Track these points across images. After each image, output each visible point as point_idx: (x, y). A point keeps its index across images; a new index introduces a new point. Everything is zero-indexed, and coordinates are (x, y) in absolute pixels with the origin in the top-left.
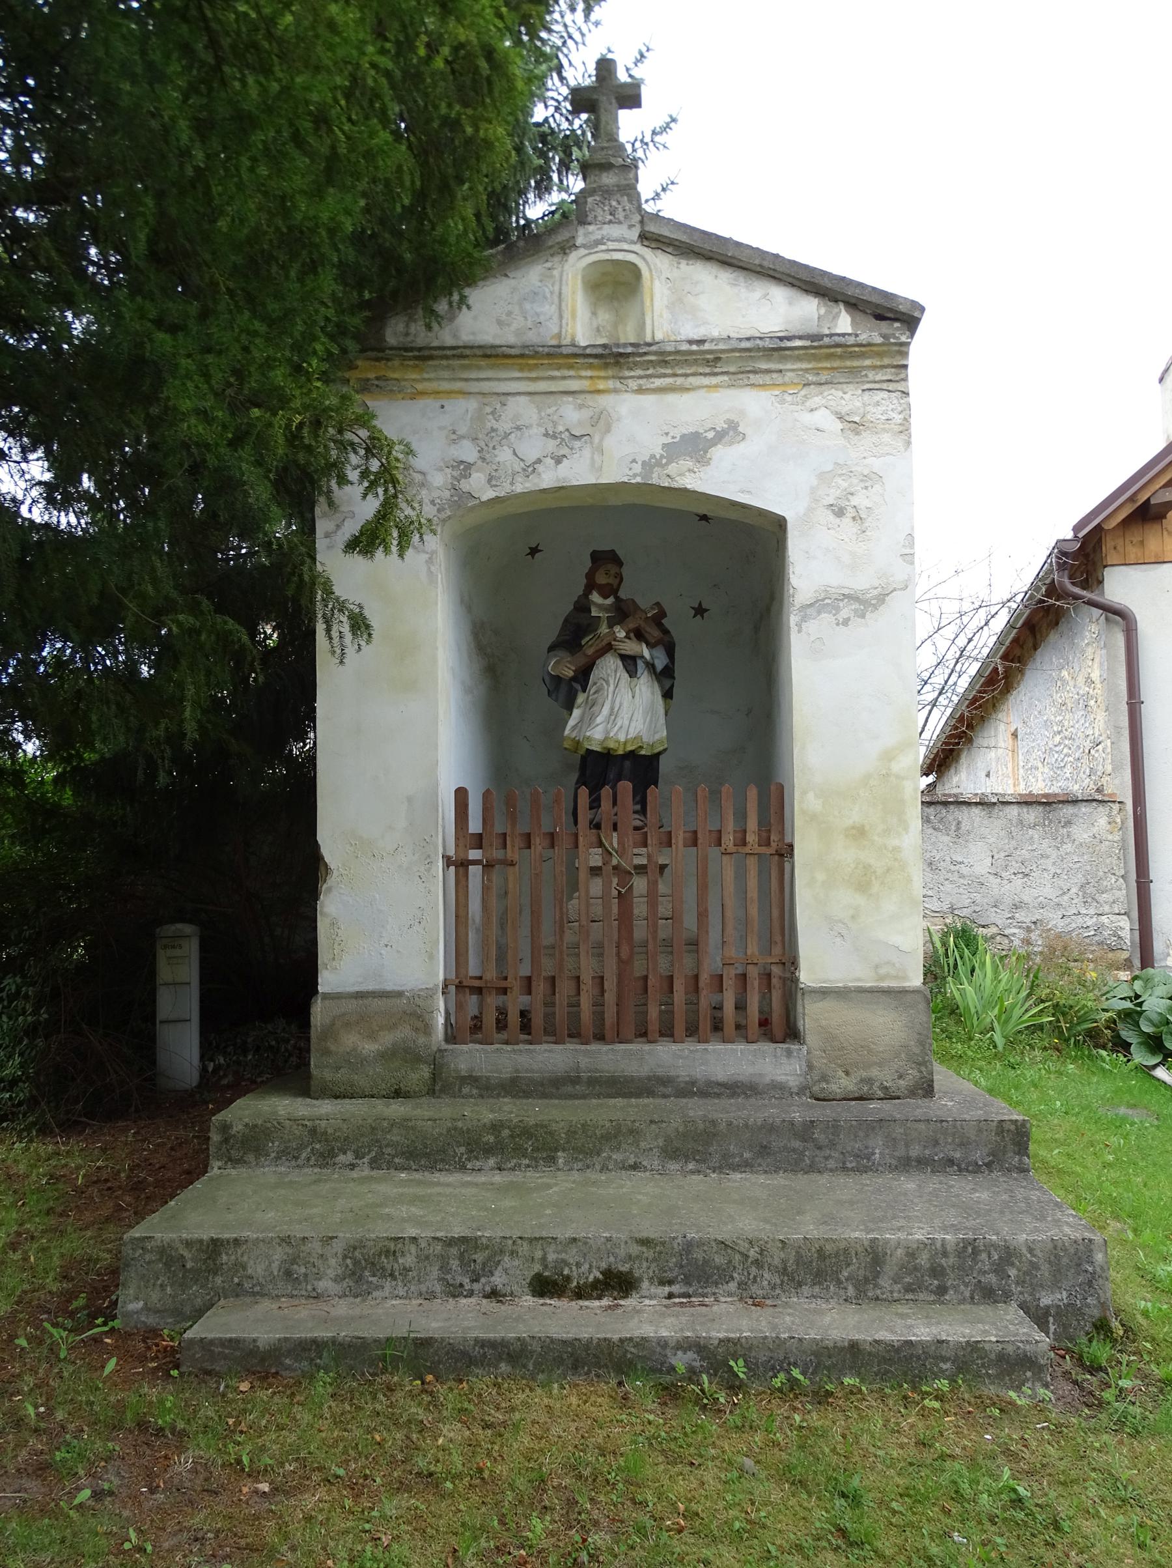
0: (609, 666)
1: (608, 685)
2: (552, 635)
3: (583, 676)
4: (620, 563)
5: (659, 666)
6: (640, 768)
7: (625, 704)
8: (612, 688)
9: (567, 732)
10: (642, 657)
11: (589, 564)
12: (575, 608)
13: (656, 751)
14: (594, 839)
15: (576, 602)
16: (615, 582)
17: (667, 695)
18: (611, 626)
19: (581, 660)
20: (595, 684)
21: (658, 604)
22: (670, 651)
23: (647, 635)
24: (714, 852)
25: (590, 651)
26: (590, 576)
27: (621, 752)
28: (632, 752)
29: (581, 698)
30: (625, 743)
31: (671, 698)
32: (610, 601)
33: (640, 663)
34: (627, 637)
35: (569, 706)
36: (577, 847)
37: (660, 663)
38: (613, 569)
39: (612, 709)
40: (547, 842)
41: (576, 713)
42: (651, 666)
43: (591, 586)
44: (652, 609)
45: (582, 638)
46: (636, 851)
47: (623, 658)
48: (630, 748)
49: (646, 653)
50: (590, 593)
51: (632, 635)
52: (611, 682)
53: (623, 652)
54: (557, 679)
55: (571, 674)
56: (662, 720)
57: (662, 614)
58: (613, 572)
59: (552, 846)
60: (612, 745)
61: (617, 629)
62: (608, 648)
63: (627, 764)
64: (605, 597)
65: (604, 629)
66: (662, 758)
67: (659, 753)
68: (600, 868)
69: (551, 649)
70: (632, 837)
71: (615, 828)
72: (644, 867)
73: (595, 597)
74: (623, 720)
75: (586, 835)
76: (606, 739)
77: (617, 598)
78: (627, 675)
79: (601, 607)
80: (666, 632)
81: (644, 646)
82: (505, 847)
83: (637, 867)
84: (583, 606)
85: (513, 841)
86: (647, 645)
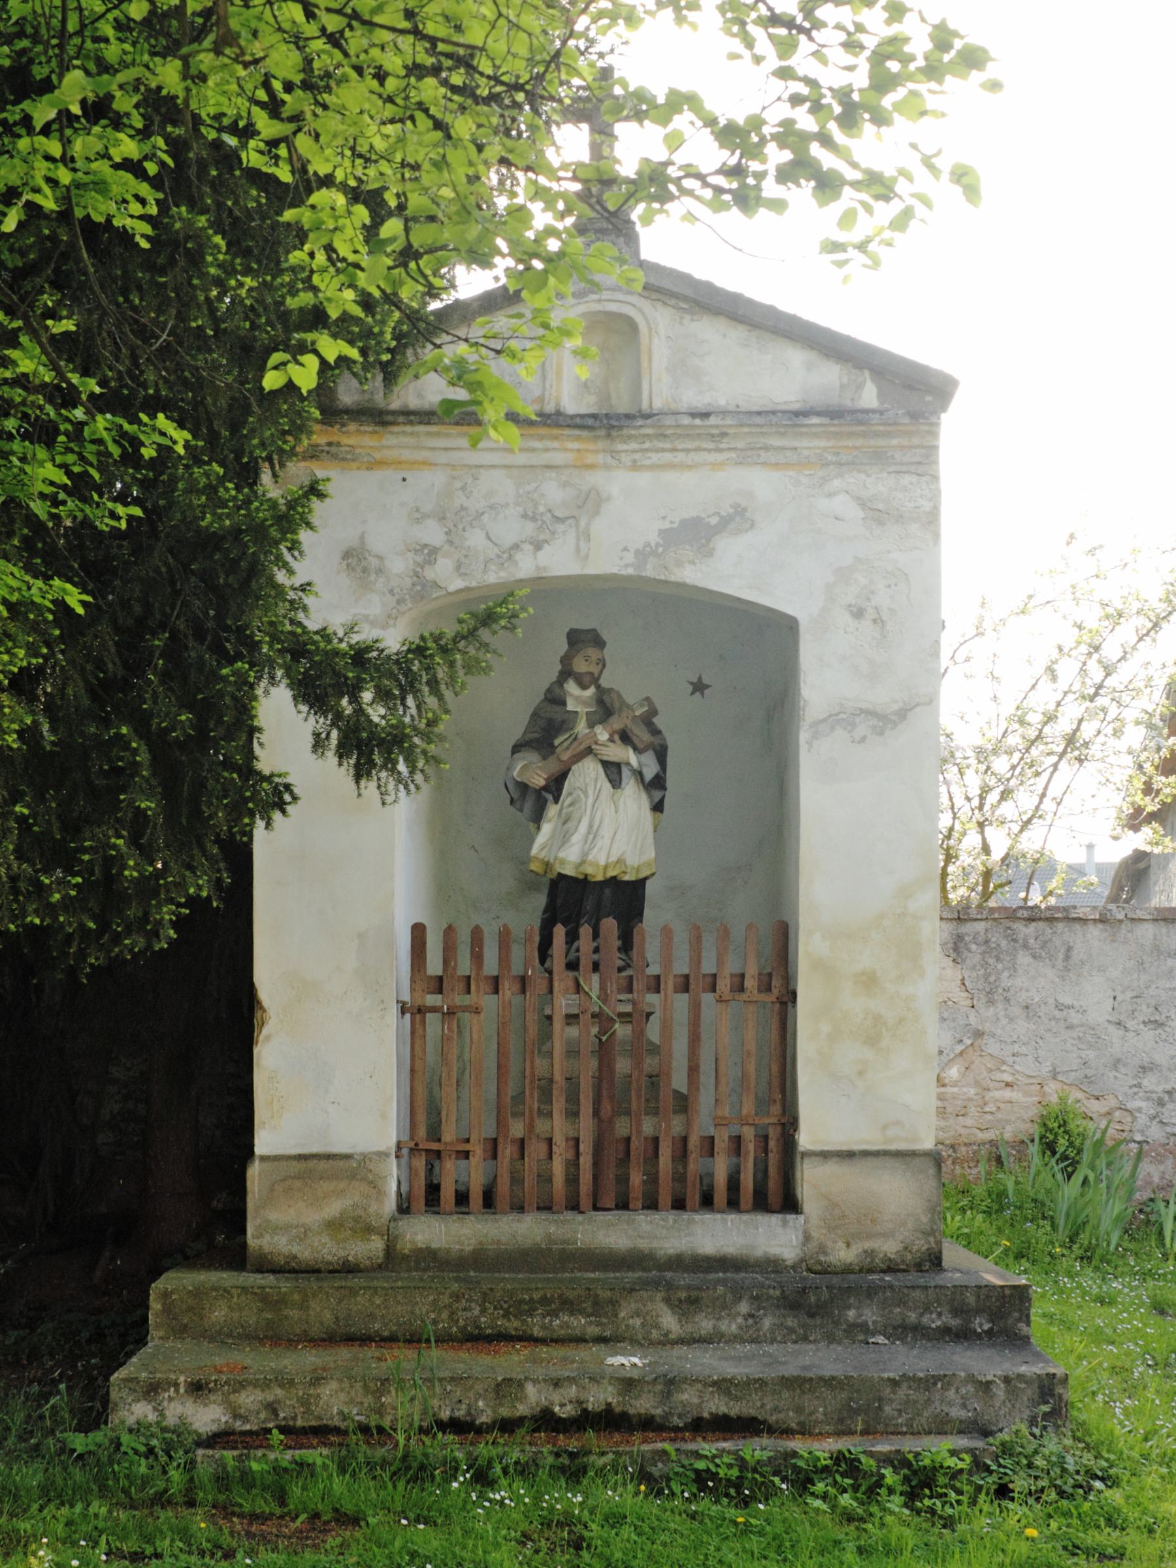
0: (587, 776)
1: (587, 797)
2: (517, 733)
3: (556, 785)
4: (599, 643)
5: (649, 774)
6: (624, 898)
7: (606, 821)
8: (590, 801)
9: (534, 851)
10: (628, 764)
11: (565, 647)
12: (546, 699)
13: (642, 875)
14: (571, 984)
15: (549, 691)
16: (595, 670)
17: (658, 807)
18: (591, 725)
19: (553, 766)
20: (570, 794)
21: (648, 699)
22: (661, 755)
23: (634, 739)
24: (707, 998)
25: (565, 757)
26: (566, 660)
27: (600, 878)
28: (614, 878)
29: (552, 810)
30: (606, 867)
31: (661, 811)
32: (591, 691)
33: (625, 772)
34: (611, 740)
35: (538, 817)
36: (551, 991)
37: (651, 769)
38: (593, 653)
39: (591, 826)
40: (516, 987)
41: (547, 828)
42: (639, 774)
43: (567, 673)
44: (642, 706)
45: (556, 737)
46: (621, 997)
47: (606, 764)
48: (611, 873)
49: (633, 759)
50: (565, 680)
51: (616, 737)
52: (590, 792)
53: (605, 758)
54: (523, 787)
55: (542, 783)
56: (650, 840)
57: (653, 712)
58: (594, 658)
59: (523, 991)
60: (589, 870)
61: (599, 729)
62: (589, 751)
63: (607, 892)
64: (584, 687)
65: (581, 727)
66: (648, 883)
67: (646, 879)
68: (576, 1016)
69: (516, 748)
70: (615, 981)
71: (596, 967)
72: (629, 1015)
73: (571, 687)
74: (603, 842)
75: (562, 980)
76: (583, 862)
77: (598, 687)
78: (608, 785)
79: (577, 699)
80: (656, 732)
81: (631, 751)
82: (469, 992)
83: (621, 1015)
84: (555, 698)
85: (478, 986)
86: (635, 749)
